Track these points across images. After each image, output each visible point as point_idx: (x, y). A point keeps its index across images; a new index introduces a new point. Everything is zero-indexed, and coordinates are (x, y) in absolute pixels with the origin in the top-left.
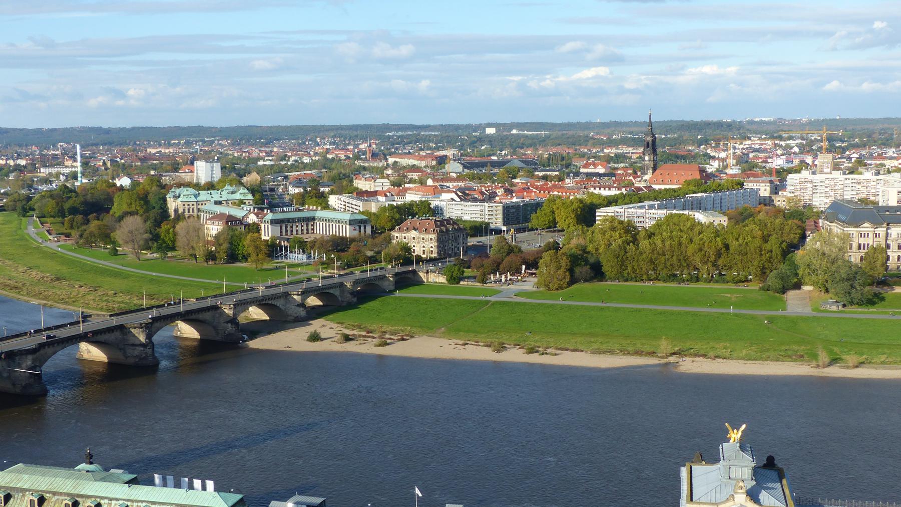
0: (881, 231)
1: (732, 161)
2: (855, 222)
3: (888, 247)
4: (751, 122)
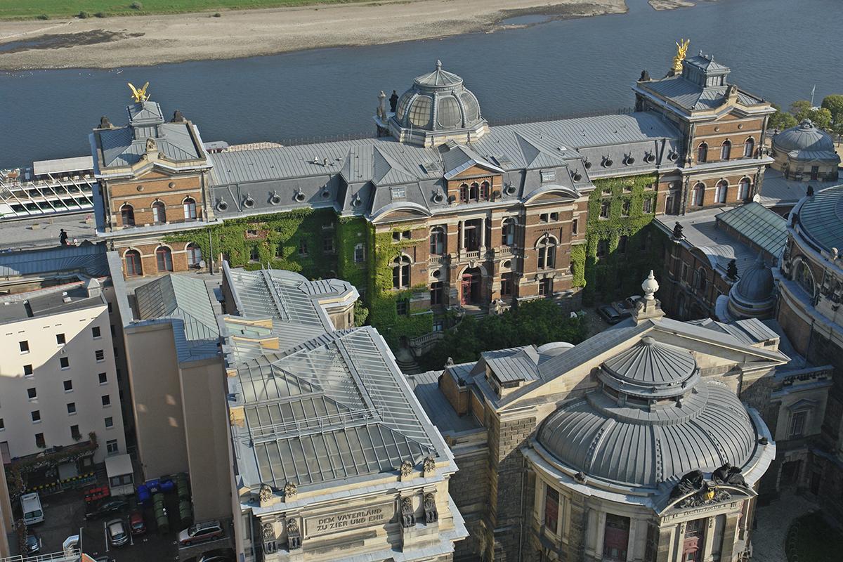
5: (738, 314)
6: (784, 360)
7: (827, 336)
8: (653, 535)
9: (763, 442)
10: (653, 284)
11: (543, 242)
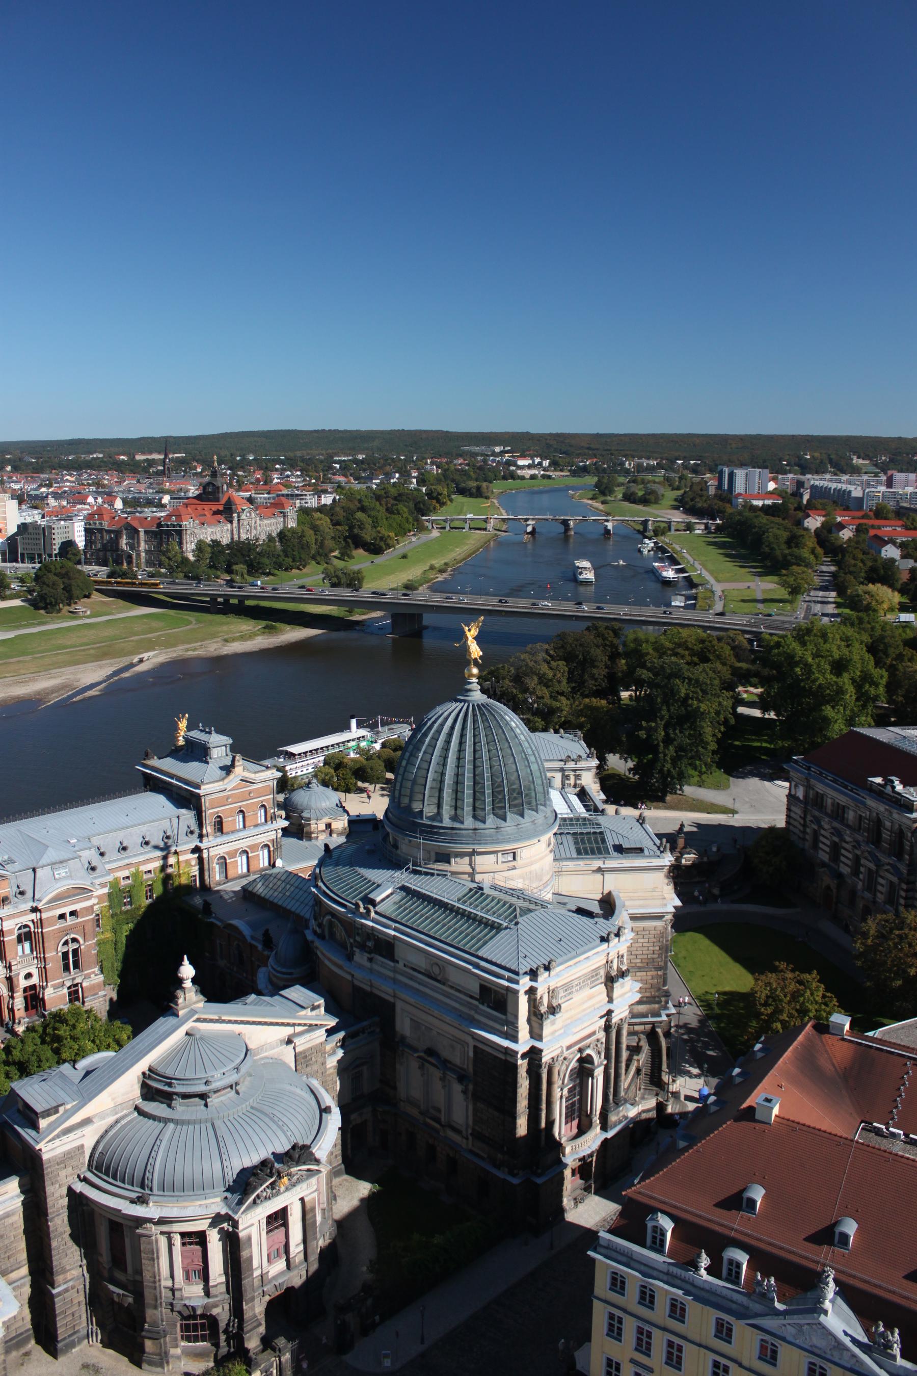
5: (281, 984)
6: (332, 1022)
7: (368, 988)
8: (233, 1244)
9: (327, 1110)
10: (187, 971)
11: (66, 943)
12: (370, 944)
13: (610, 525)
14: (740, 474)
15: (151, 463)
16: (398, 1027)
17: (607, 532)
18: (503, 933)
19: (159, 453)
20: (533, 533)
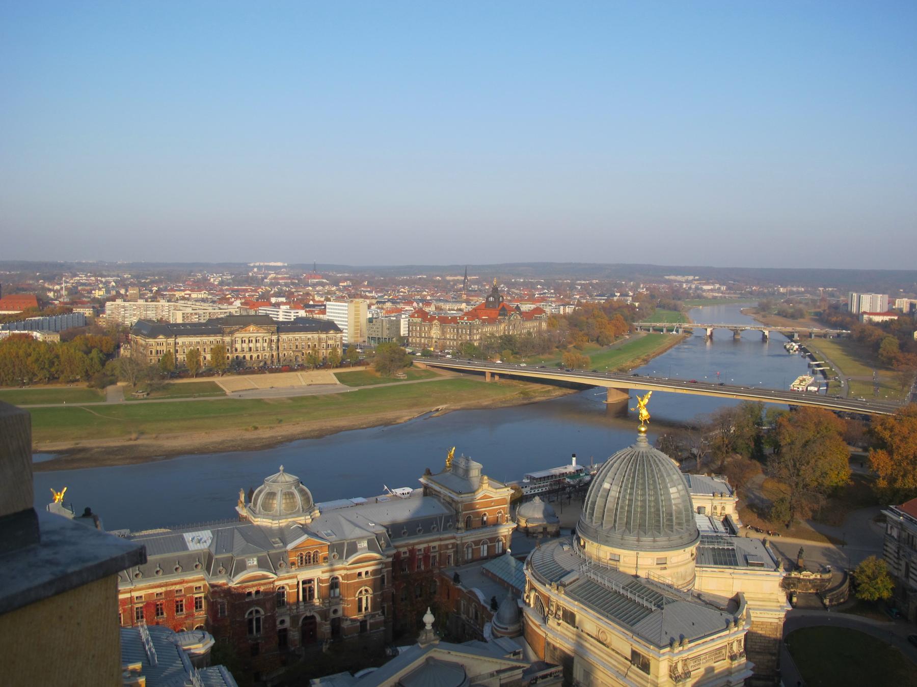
0: (171, 341)
1: (64, 292)
2: (153, 334)
3: (177, 351)
4: (80, 264)
12: (560, 613)
13: (767, 333)
14: (866, 299)
15: (456, 282)
16: (574, 676)
17: (764, 338)
18: (652, 615)
19: (461, 275)
20: (711, 336)
